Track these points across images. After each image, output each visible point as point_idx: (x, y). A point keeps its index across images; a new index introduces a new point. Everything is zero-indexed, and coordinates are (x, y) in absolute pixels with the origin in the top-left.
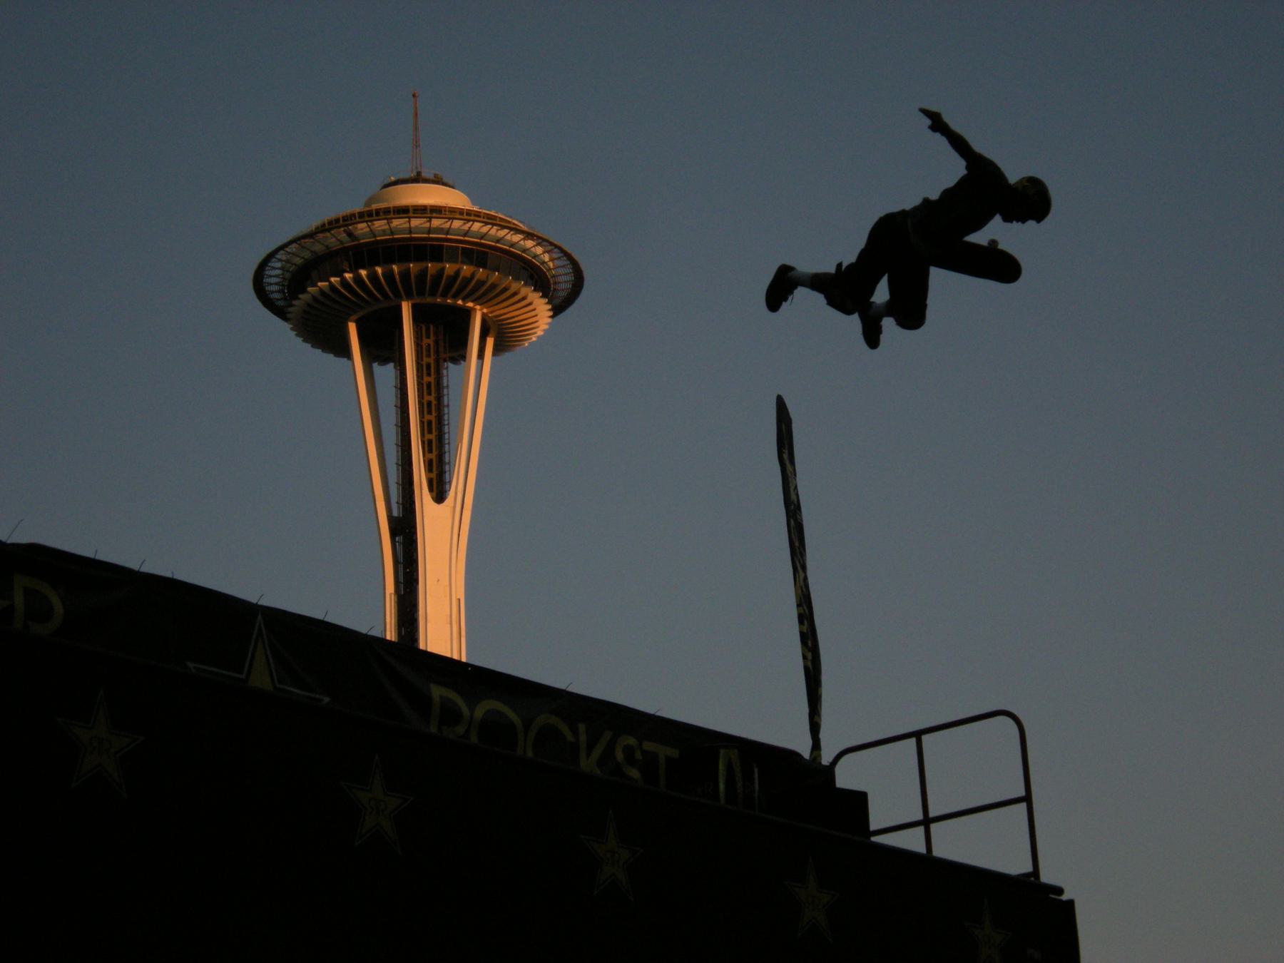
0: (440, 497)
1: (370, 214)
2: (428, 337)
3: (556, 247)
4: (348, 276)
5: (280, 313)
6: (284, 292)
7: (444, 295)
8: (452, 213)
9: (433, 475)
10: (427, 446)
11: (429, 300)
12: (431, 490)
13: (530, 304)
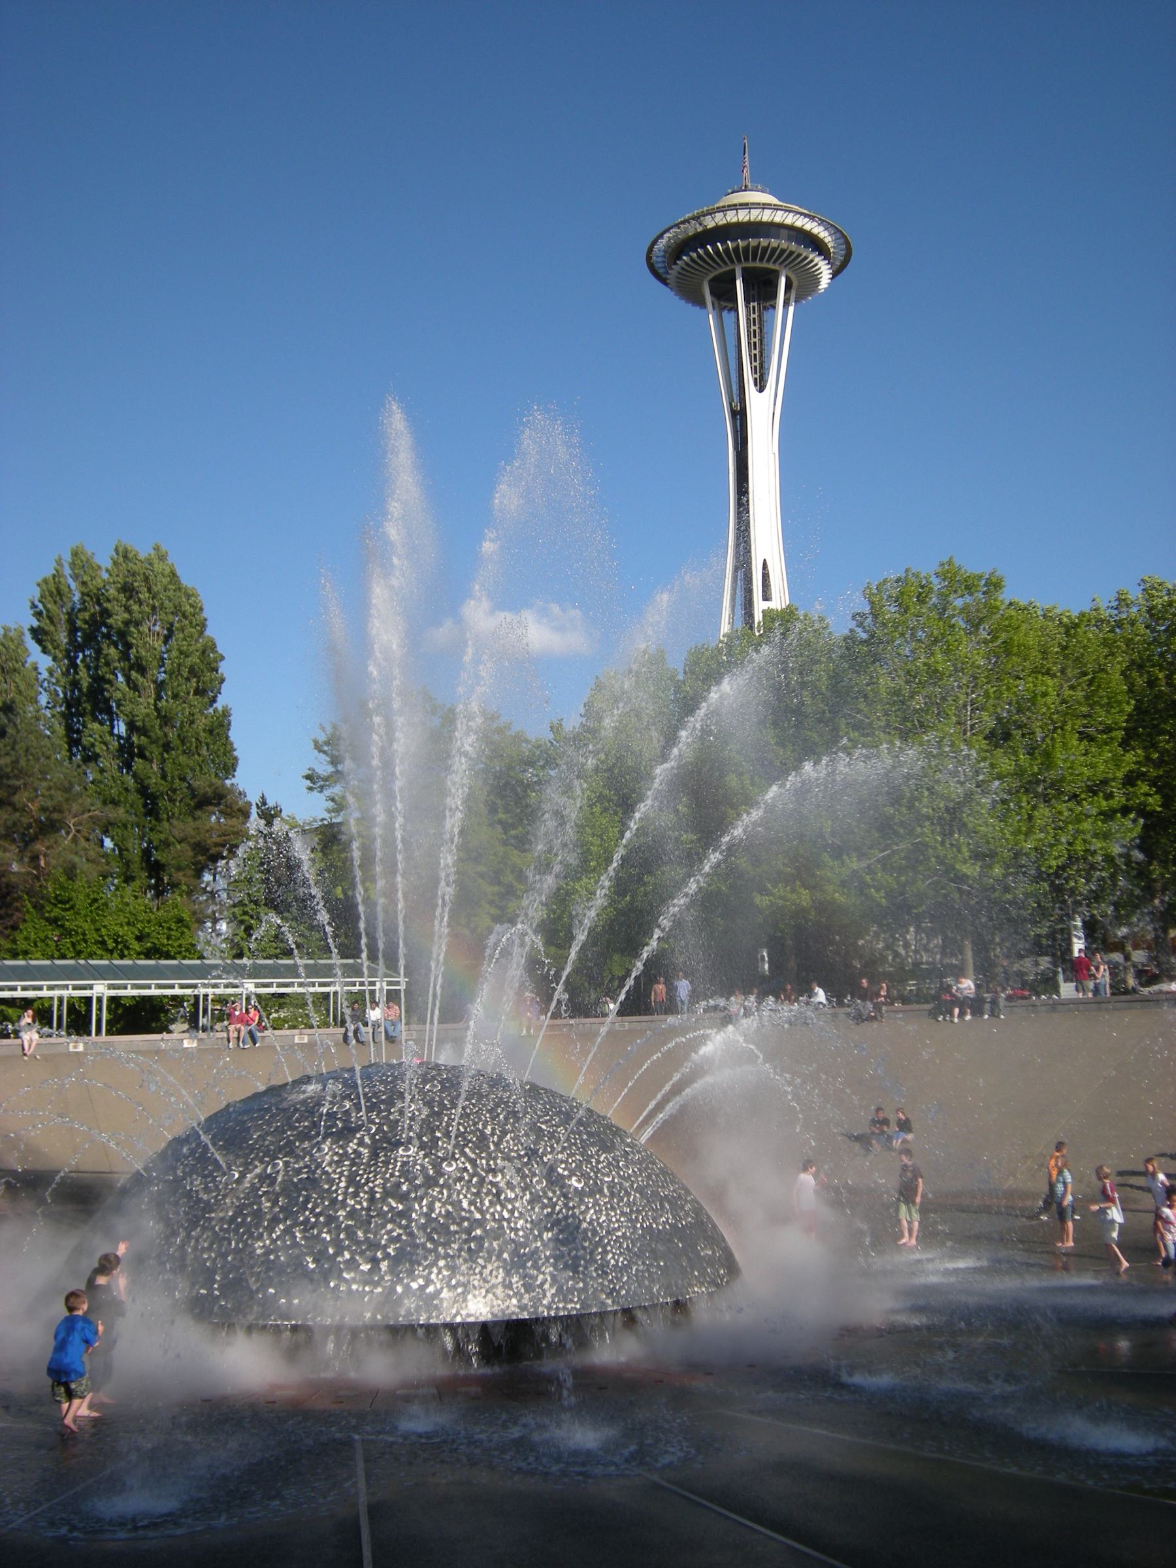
0: (761, 390)
2: (753, 289)
3: (832, 225)
5: (664, 281)
7: (761, 260)
8: (764, 206)
9: (757, 376)
10: (753, 358)
11: (751, 264)
12: (756, 385)
13: (816, 265)
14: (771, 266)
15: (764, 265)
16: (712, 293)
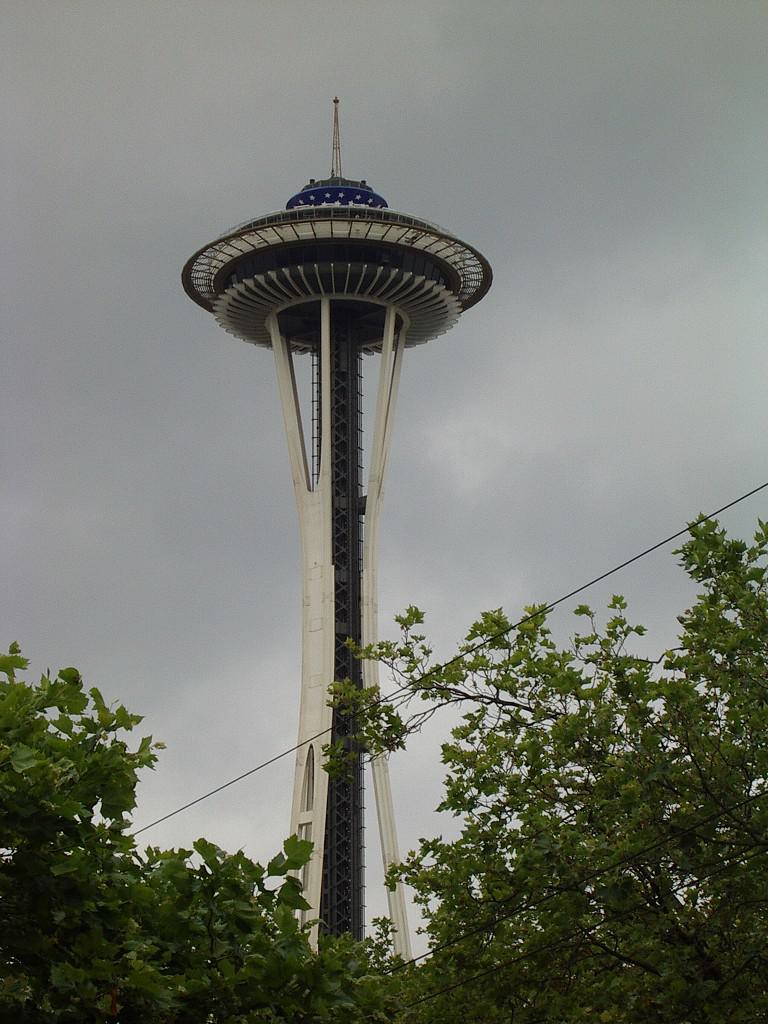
1: (293, 216)
4: (273, 274)
5: (208, 306)
6: (210, 286)
7: (361, 292)
11: (345, 296)
13: (442, 301)
14: (375, 301)
15: (366, 299)
16: (282, 332)
